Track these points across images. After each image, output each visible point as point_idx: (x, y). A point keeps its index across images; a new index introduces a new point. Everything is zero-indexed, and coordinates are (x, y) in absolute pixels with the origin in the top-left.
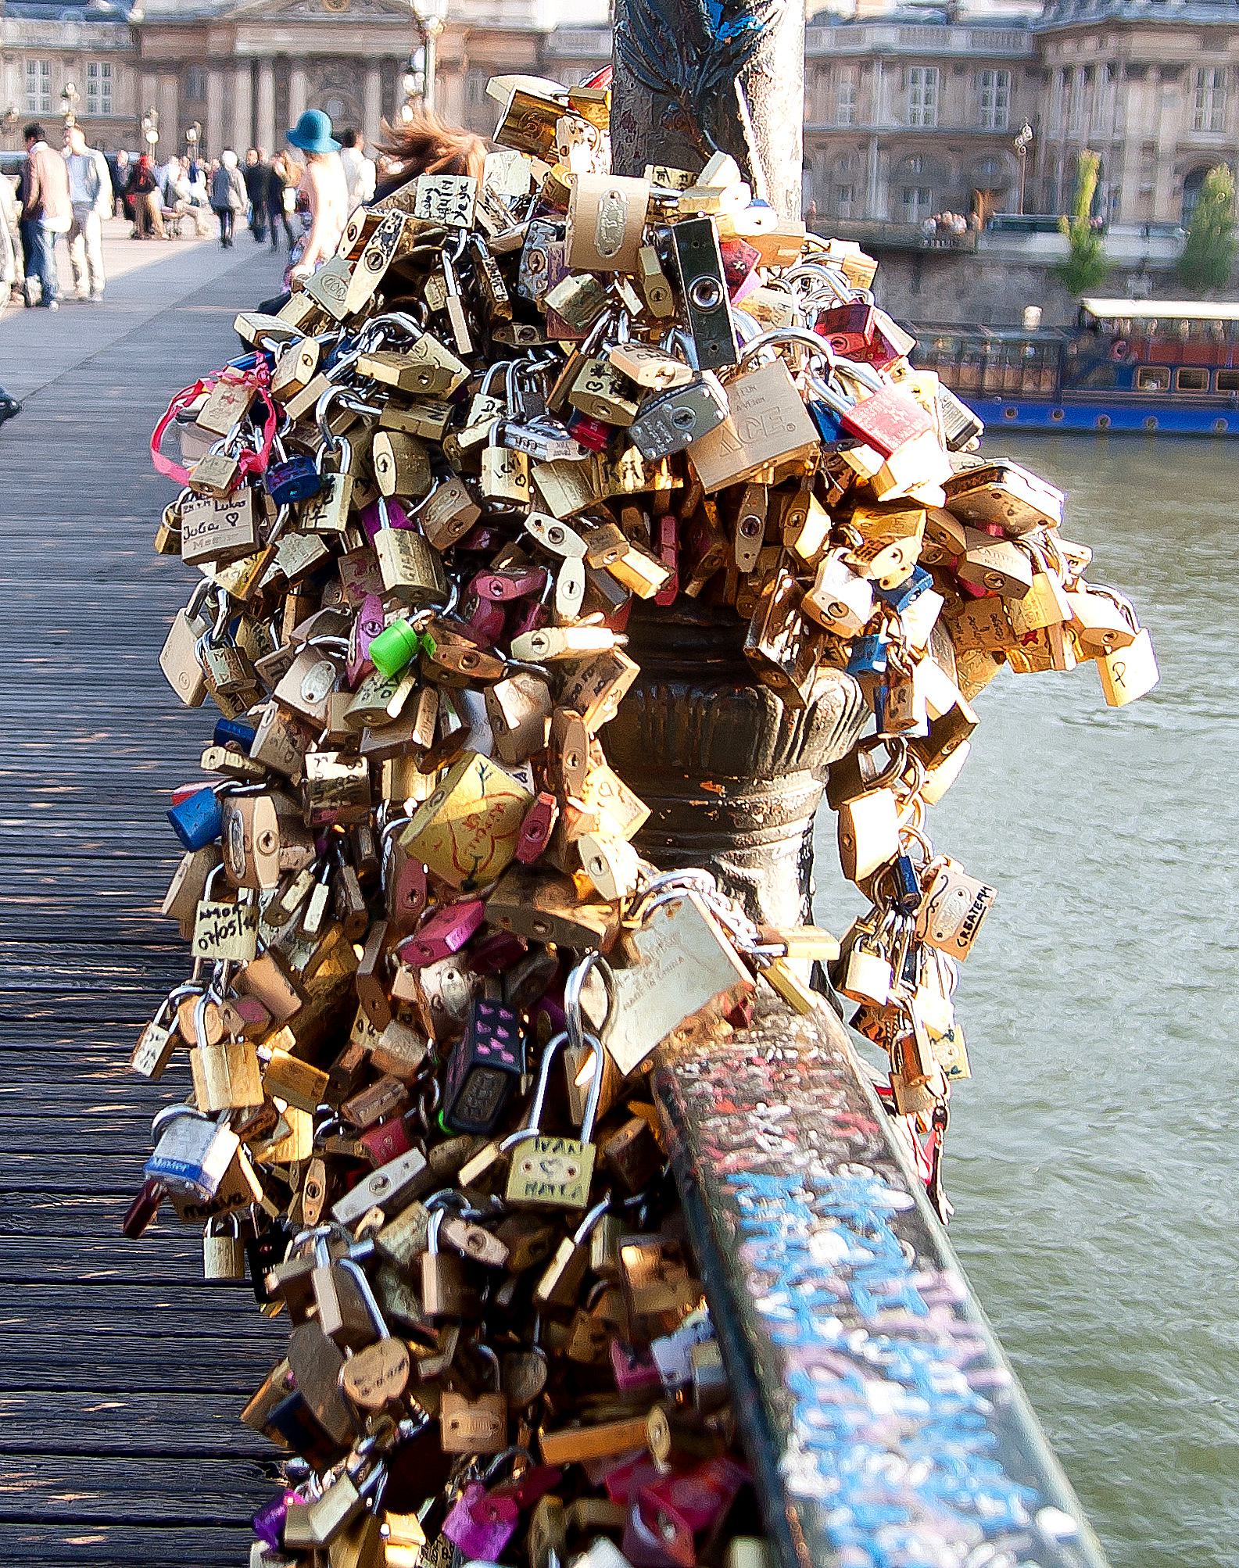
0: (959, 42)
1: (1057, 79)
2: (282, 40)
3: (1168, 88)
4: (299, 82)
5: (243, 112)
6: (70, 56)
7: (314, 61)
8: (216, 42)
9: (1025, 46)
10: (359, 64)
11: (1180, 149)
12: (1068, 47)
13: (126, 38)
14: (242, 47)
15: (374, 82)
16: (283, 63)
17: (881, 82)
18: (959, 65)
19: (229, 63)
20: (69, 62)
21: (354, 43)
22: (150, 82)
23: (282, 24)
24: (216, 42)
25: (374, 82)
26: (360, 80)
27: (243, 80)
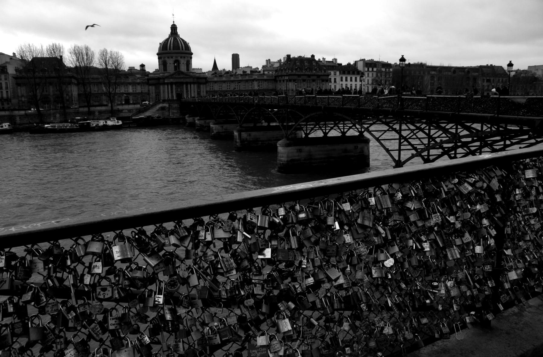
0: (265, 77)
1: (279, 82)
2: (171, 80)
4: (174, 86)
5: (166, 91)
6: (139, 84)
7: (176, 83)
8: (161, 81)
9: (274, 78)
12: (280, 78)
13: (146, 81)
14: (166, 81)
15: (185, 86)
16: (172, 84)
17: (256, 83)
18: (266, 80)
19: (164, 84)
21: (182, 80)
22: (150, 87)
23: (172, 78)
24: (161, 81)
25: (185, 86)
27: (166, 86)
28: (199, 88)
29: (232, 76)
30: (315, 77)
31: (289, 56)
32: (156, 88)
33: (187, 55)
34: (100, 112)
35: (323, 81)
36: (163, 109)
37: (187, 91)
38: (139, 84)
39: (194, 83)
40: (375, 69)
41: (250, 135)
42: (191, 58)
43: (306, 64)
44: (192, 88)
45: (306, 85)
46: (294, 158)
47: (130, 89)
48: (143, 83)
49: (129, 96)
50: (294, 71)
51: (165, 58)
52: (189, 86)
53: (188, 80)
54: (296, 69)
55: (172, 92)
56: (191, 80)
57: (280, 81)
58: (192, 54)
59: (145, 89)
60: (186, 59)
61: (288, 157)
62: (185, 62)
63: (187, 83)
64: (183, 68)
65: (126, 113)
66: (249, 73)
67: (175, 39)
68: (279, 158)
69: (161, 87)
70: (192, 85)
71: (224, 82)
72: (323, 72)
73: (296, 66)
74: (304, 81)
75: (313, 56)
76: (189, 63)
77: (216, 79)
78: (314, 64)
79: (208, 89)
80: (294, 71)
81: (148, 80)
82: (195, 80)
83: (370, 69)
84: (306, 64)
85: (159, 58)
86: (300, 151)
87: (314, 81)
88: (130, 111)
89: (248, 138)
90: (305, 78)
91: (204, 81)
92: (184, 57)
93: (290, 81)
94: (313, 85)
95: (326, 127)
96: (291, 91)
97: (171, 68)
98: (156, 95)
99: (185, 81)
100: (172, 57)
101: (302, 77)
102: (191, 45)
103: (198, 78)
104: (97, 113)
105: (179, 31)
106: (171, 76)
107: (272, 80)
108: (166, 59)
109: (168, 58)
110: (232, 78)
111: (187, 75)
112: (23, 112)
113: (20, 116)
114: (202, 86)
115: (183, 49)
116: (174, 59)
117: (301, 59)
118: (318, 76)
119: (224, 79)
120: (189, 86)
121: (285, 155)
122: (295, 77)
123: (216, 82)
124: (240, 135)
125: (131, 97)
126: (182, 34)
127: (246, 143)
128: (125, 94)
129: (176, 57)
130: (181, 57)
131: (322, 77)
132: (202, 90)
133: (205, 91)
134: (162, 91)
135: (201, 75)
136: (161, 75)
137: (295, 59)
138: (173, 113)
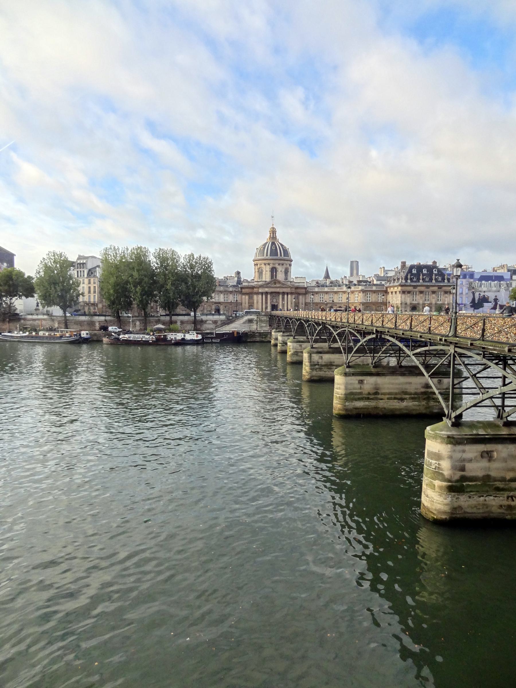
0: (374, 288)
2: (267, 290)
3: (409, 295)
5: (260, 301)
6: (231, 292)
7: (271, 293)
10: (279, 293)
11: (411, 304)
12: (392, 289)
13: (240, 289)
14: (260, 291)
16: (267, 293)
18: (374, 292)
19: (258, 293)
20: (231, 293)
21: (278, 290)
23: (267, 287)
24: (255, 290)
25: (281, 296)
26: (279, 296)
27: (260, 296)
28: (297, 298)
29: (335, 286)
30: (435, 289)
31: (404, 264)
32: (250, 298)
33: (286, 262)
34: (182, 322)
35: (446, 292)
36: (250, 321)
38: (231, 292)
39: (292, 293)
41: (321, 358)
42: (290, 265)
43: (425, 271)
44: (289, 299)
45: (424, 299)
46: (355, 391)
47: (221, 298)
48: (236, 292)
49: (219, 305)
50: (409, 281)
51: (261, 264)
52: (286, 296)
53: (285, 290)
54: (411, 279)
55: (266, 303)
57: (392, 292)
58: (291, 261)
59: (239, 297)
60: (285, 266)
61: (346, 389)
62: (283, 270)
63: (283, 293)
64: (280, 276)
65: (210, 324)
66: (356, 283)
67: (273, 243)
68: (335, 390)
69: (255, 297)
70: (289, 296)
71: (327, 293)
72: (446, 281)
73: (412, 274)
74: (421, 292)
75: (435, 262)
76: (287, 272)
77: (316, 289)
78: (435, 272)
79: (308, 301)
80: (409, 281)
81: (242, 288)
82: (293, 290)
84: (425, 271)
85: (255, 265)
86: (361, 382)
87: (434, 292)
88: (215, 322)
89: (320, 361)
90: (422, 289)
91: (303, 291)
92: (283, 264)
93: (404, 292)
94: (433, 298)
95: (400, 353)
96: (404, 305)
97: (267, 277)
98: (250, 306)
99: (281, 290)
100: (269, 264)
101: (419, 288)
102: (290, 251)
103: (297, 288)
104: (179, 323)
105: (278, 235)
106: (266, 285)
107: (383, 291)
108: (263, 266)
109: (265, 264)
110: (336, 289)
111: (284, 284)
114: (301, 297)
115: (281, 255)
116: (271, 266)
117: (420, 268)
118: (440, 287)
119: (326, 289)
120: (286, 296)
121: (343, 387)
122: (410, 289)
123: (317, 293)
124: (310, 357)
125: (222, 307)
126: (282, 238)
127: (317, 366)
128: (216, 303)
129: (273, 264)
130: (279, 264)
131: (444, 288)
132: (300, 301)
133: (304, 303)
134: (255, 301)
135: (300, 284)
136: (256, 283)
137: (412, 267)
138: (261, 327)
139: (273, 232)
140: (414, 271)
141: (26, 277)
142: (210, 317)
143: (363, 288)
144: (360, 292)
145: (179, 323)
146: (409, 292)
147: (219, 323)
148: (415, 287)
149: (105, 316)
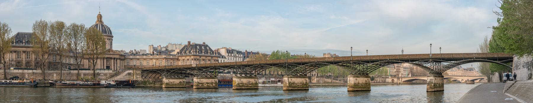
7: (107, 58)
10: (111, 58)
16: (104, 59)
18: (172, 59)
21: (111, 56)
30: (210, 58)
37: (114, 65)
40: (232, 55)
55: (104, 65)
56: (117, 57)
63: (114, 58)
76: (111, 44)
77: (131, 57)
83: (230, 55)
93: (195, 59)
104: (82, 75)
105: (103, 20)
112: (30, 71)
113: (29, 74)
139: (100, 17)
140: (198, 47)
141: (12, 34)
142: (103, 71)
143: (165, 56)
144: (163, 59)
145: (82, 75)
146: (198, 60)
147: (108, 75)
148: (200, 56)
149: (32, 69)
